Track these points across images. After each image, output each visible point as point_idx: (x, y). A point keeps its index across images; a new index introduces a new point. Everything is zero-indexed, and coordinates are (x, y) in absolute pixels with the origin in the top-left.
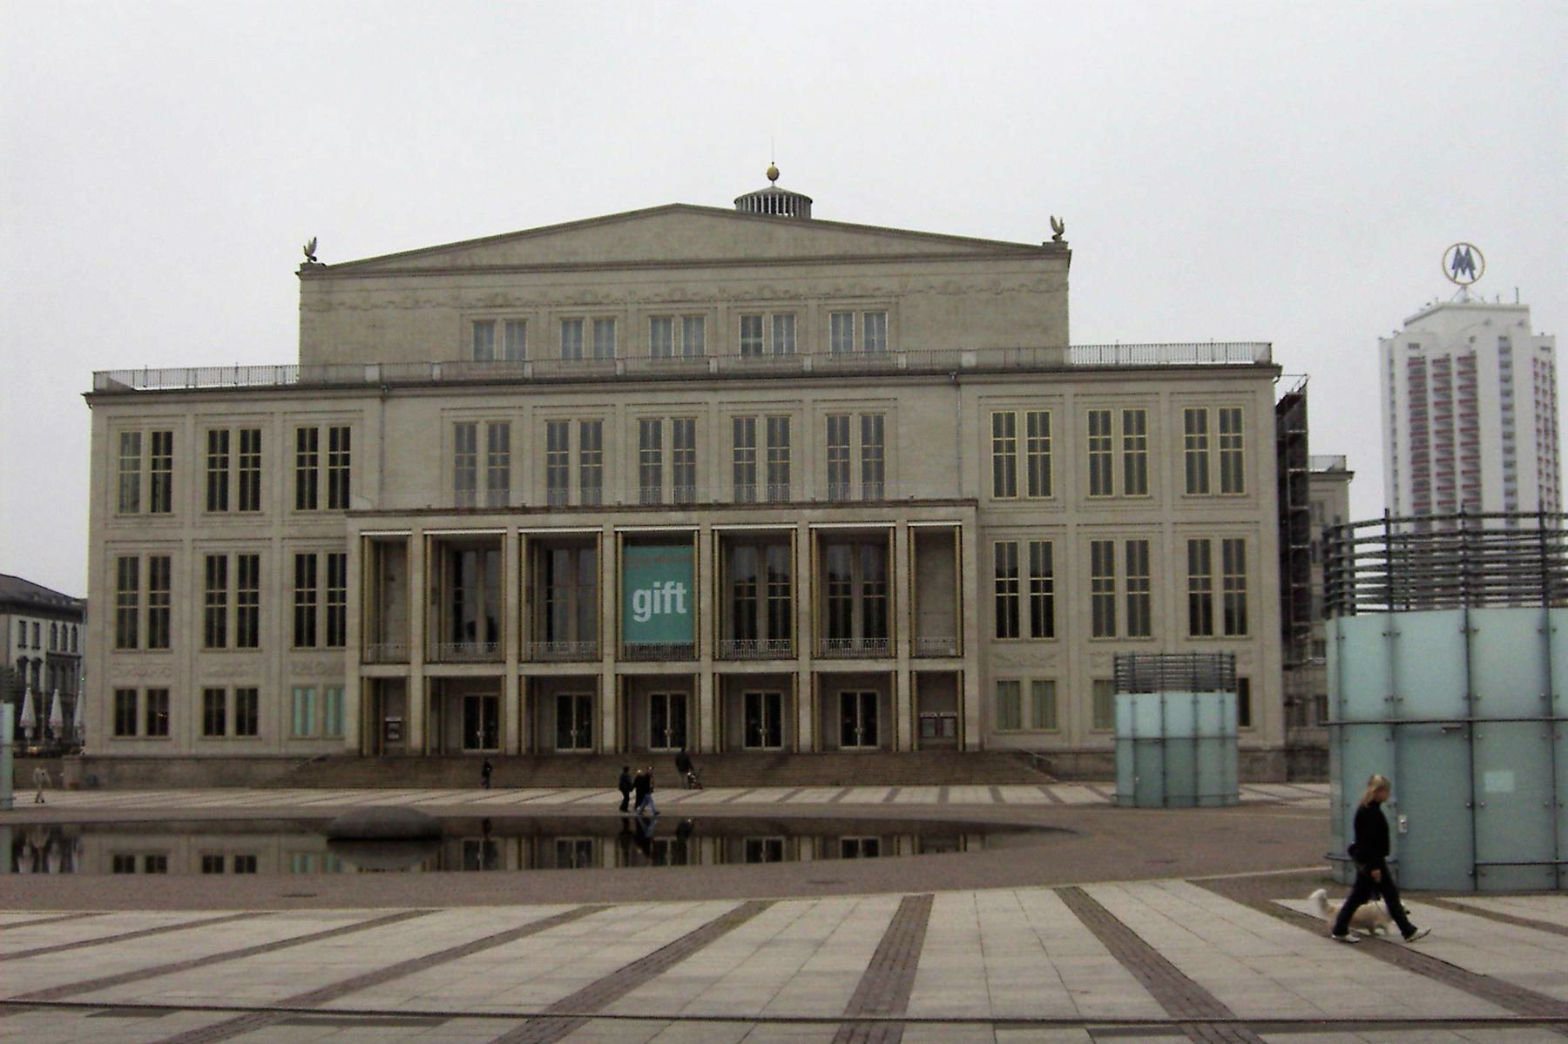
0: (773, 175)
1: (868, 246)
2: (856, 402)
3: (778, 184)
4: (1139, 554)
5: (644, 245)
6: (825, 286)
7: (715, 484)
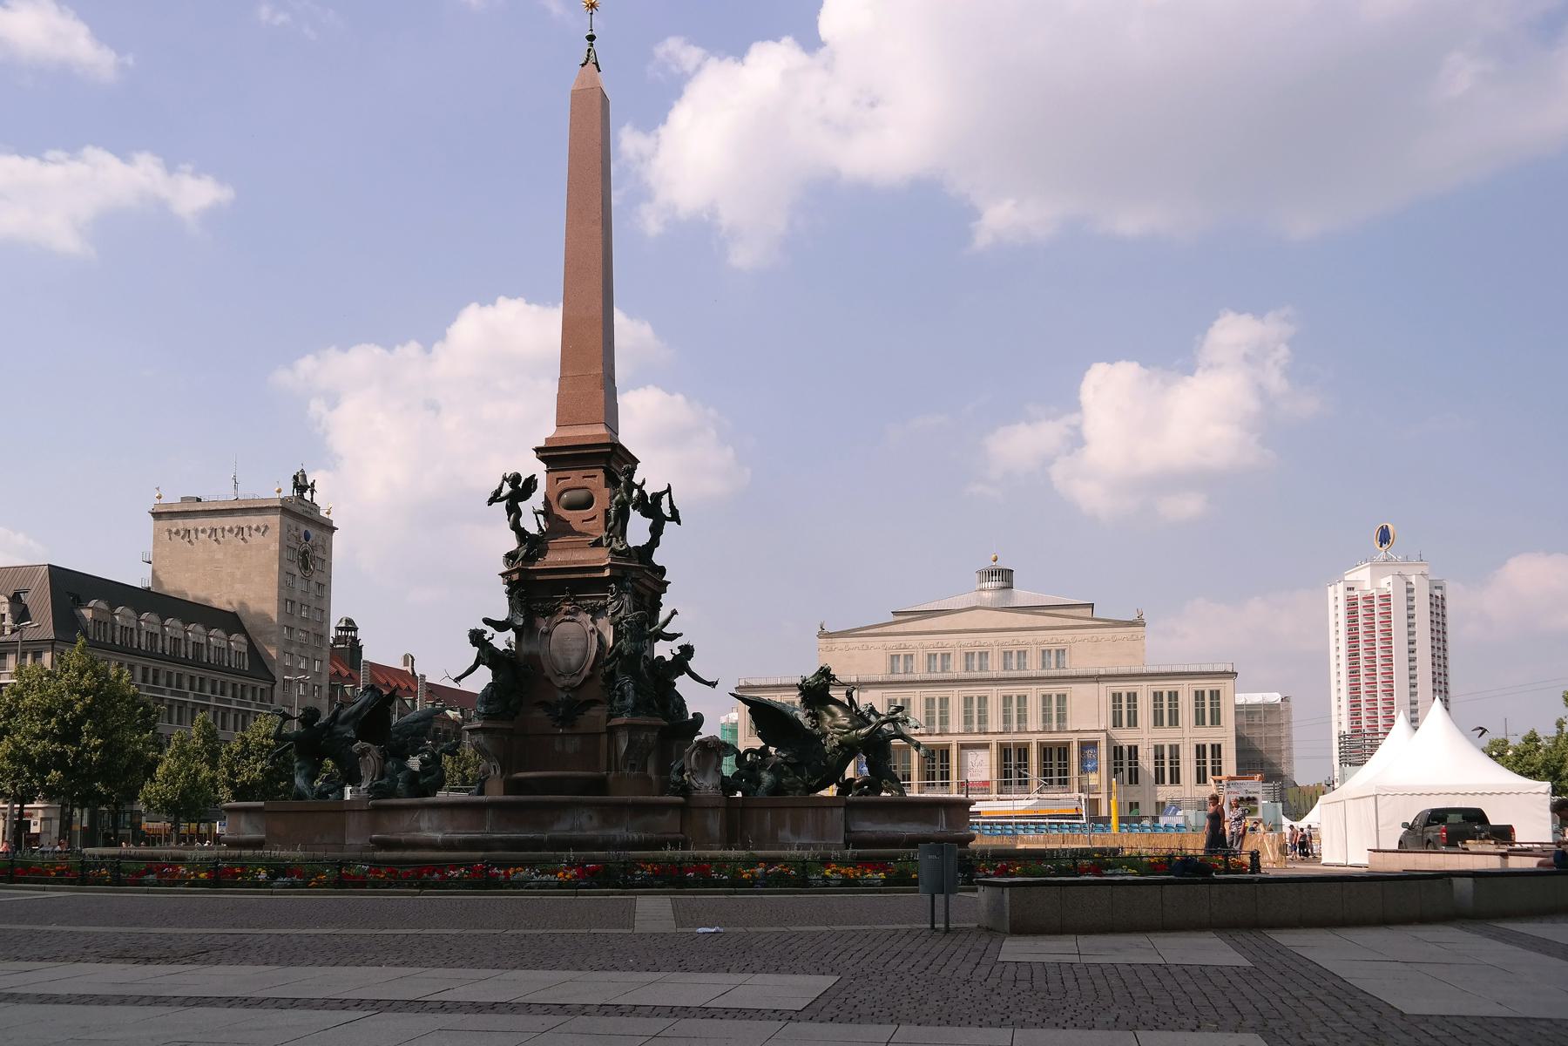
2: (1054, 690)
4: (1175, 749)
6: (1040, 639)
7: (995, 723)
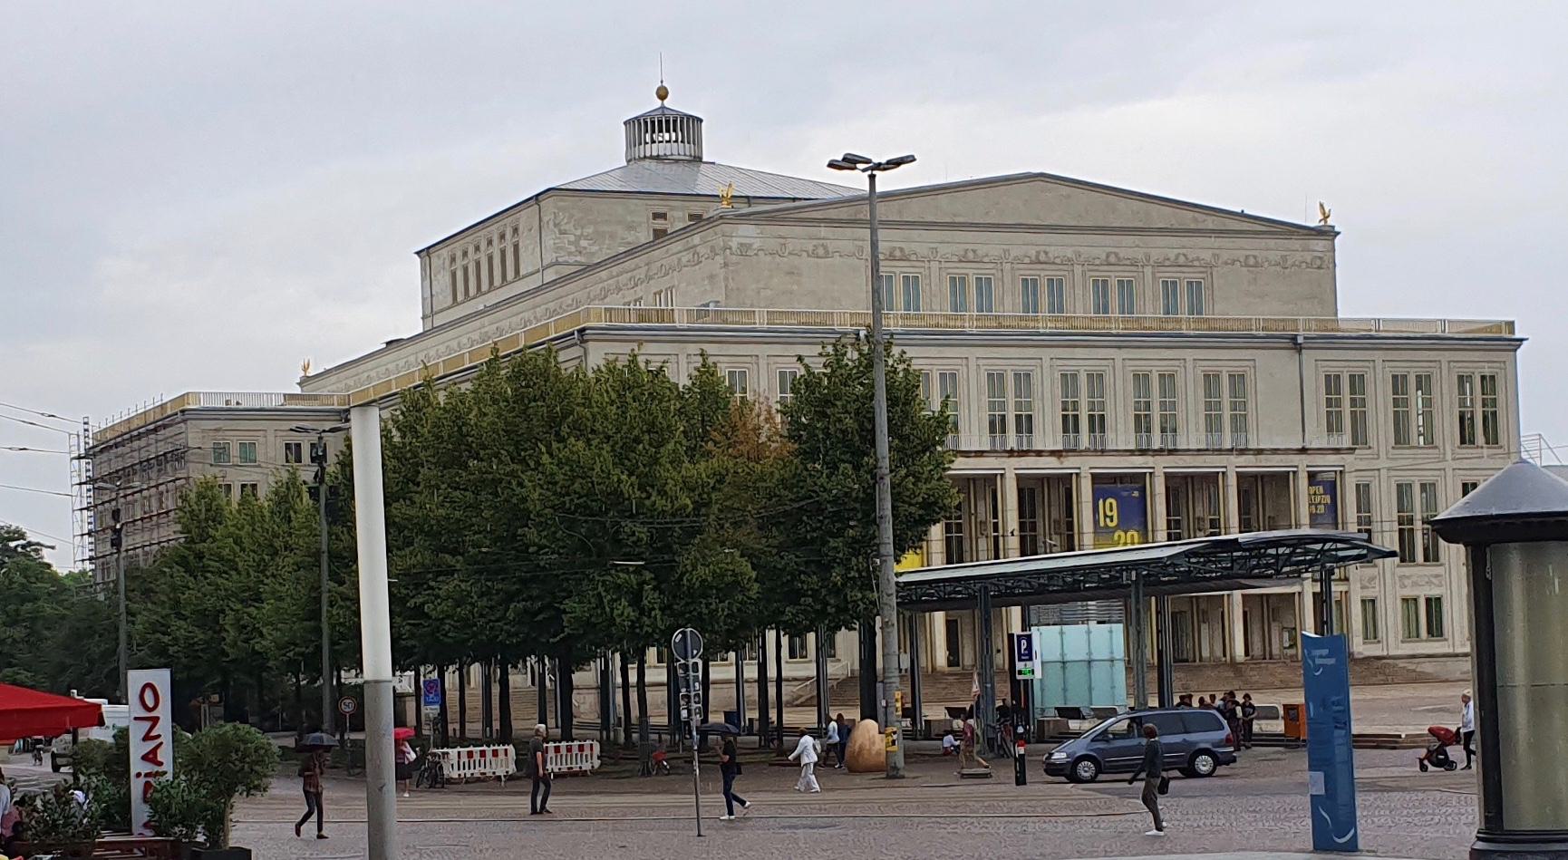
0: (662, 93)
1: (1187, 218)
2: (1225, 361)
3: (667, 103)
5: (1013, 207)
6: (1156, 255)
